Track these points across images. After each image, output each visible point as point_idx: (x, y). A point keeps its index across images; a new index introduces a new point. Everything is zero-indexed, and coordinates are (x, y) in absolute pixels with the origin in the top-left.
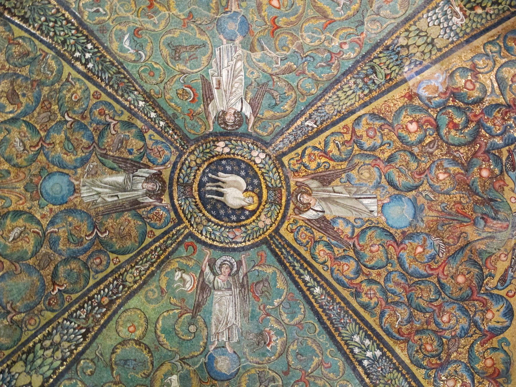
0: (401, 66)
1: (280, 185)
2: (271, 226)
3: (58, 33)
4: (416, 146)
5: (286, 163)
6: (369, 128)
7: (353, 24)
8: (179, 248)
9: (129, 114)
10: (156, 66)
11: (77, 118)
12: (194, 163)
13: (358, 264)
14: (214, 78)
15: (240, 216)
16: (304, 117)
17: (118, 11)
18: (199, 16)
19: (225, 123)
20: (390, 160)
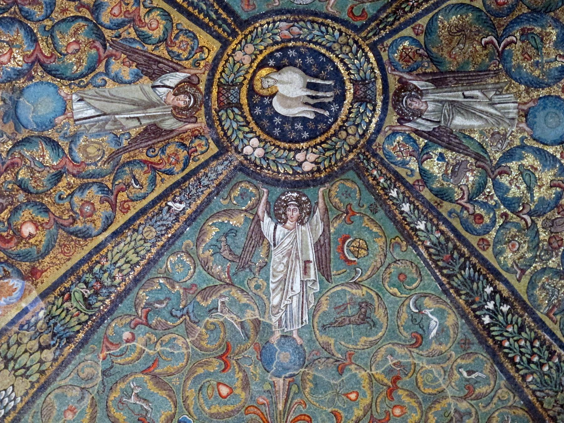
0: (50, 316)
1: (220, 114)
2: (234, 50)
3: (528, 344)
4: (22, 203)
5: (213, 145)
6: (91, 215)
7: (117, 370)
8: (375, 12)
9: (440, 210)
10: (395, 290)
11: (515, 216)
12: (350, 131)
13: (97, 19)
14: (312, 278)
15: (283, 57)
16: (186, 216)
17: (442, 373)
18: (330, 369)
19: (300, 205)
20: (58, 176)
